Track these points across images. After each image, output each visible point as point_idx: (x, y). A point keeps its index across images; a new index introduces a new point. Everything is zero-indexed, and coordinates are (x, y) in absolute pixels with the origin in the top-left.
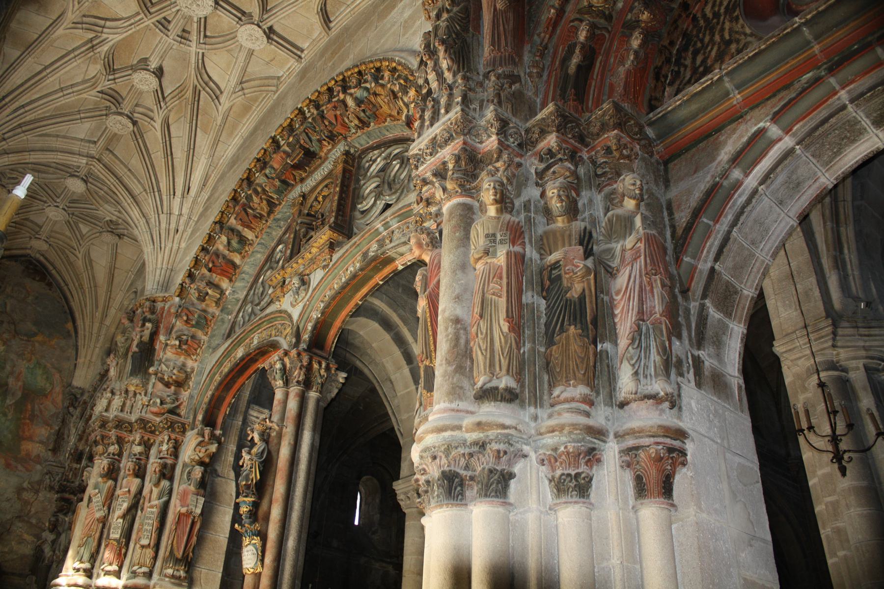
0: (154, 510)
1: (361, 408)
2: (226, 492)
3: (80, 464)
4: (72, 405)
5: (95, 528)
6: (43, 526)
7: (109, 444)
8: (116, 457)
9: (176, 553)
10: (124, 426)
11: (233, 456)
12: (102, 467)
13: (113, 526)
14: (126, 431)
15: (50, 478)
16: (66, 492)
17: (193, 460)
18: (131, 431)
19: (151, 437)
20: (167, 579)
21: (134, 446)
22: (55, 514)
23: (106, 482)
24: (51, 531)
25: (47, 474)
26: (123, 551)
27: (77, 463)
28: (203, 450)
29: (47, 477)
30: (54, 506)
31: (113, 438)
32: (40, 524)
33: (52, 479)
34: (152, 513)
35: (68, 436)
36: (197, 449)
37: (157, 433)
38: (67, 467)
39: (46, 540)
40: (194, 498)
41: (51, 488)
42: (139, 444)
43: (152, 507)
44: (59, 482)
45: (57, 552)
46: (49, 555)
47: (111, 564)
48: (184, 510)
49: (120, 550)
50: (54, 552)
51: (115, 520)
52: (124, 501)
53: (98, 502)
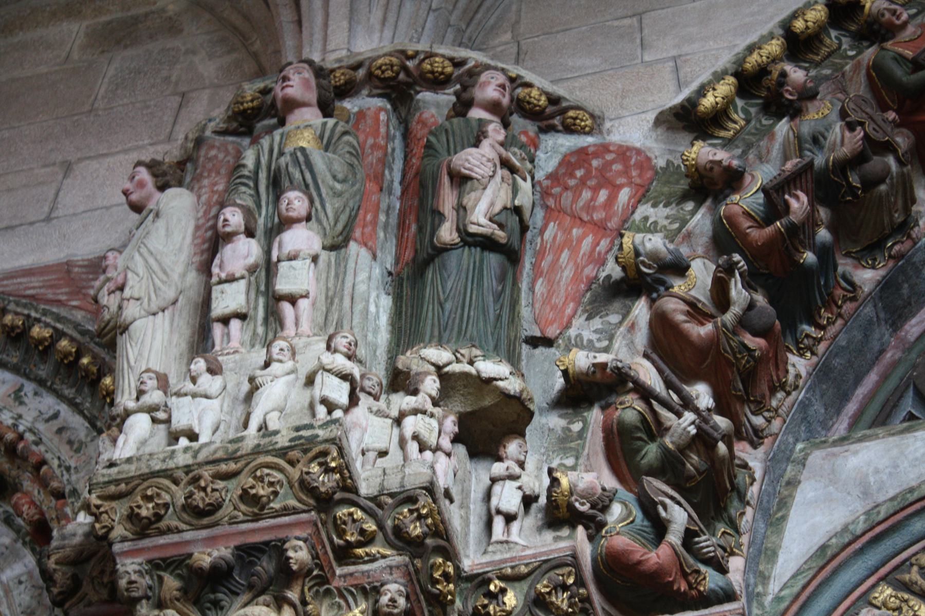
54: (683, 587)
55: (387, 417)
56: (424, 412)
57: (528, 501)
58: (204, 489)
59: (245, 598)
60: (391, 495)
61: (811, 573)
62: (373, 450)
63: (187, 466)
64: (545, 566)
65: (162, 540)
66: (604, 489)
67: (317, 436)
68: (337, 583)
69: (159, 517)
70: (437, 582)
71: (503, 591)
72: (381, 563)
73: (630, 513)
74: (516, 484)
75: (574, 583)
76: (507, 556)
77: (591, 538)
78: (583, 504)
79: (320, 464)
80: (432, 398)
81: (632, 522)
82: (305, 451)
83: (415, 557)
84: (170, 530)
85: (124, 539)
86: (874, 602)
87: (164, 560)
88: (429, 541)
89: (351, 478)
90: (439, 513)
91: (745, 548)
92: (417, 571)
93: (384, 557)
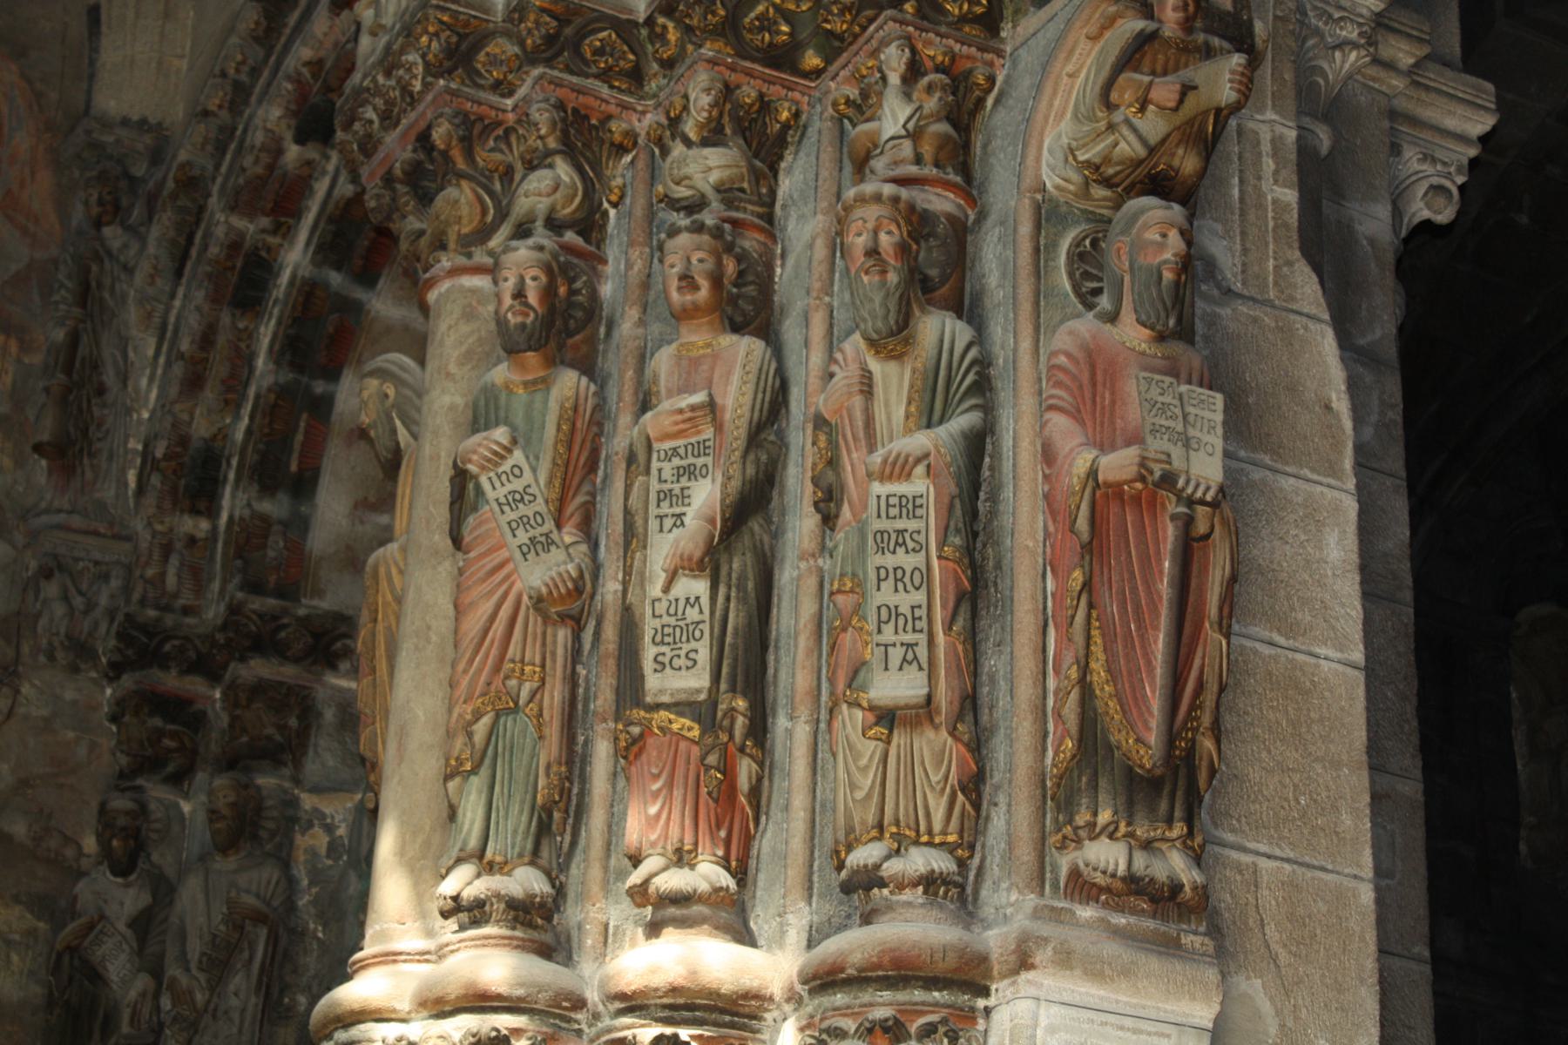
0: (918, 485)
1: (1524, 219)
2: (1293, 389)
3: (212, 513)
4: (112, 211)
5: (533, 653)
6: (70, 852)
7: (508, 174)
8: (570, 237)
9: (1121, 738)
10: (596, 40)
11: (1290, 173)
12: (509, 286)
13: (649, 626)
14: (605, 76)
15: (66, 598)
16: (163, 661)
17: (1096, 172)
18: (636, 76)
19: (775, 91)
20: (1086, 913)
21: (678, 149)
22: (124, 779)
23: (545, 383)
24: (123, 868)
25: (47, 573)
26: (745, 770)
27: (195, 512)
28: (1165, 91)
29: (51, 589)
30: (107, 743)
31: (542, 116)
32: (53, 843)
33: (78, 602)
34: (910, 506)
35: (124, 378)
36: (1125, 94)
37: (812, 60)
38: (145, 537)
39: (102, 917)
40: (1166, 391)
41: (81, 650)
43: (899, 469)
44: (111, 614)
45: (173, 971)
46: (133, 994)
47: (682, 858)
48: (1118, 464)
49: (728, 770)
50: (157, 972)
51: (655, 590)
52: (690, 472)
53: (518, 498)
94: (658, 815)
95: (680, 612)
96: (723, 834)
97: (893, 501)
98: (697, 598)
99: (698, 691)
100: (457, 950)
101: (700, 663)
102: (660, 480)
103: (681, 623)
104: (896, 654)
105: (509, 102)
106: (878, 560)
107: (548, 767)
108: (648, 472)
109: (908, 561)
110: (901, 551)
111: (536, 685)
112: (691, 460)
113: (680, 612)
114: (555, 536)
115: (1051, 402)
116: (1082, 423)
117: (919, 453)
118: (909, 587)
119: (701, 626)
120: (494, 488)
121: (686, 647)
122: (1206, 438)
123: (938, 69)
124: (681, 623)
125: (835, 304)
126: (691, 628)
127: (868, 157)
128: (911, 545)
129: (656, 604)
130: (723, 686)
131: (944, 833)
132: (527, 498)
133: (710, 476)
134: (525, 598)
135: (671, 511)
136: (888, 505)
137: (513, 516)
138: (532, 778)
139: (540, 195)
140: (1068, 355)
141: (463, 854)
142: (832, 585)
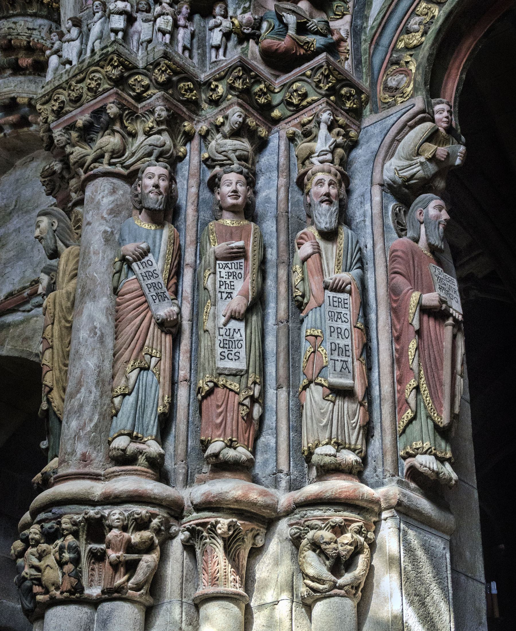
14: (184, 103)
37: (276, 113)
42: (235, 134)
47: (231, 445)
54: (302, 52)
55: (150, 21)
56: (163, 14)
57: (227, 35)
58: (73, 90)
59: (100, 134)
60: (151, 64)
61: (385, 9)
62: (145, 41)
63: (66, 81)
64: (231, 70)
65: (66, 118)
66: (255, 19)
67: (108, 51)
68: (140, 111)
69: (61, 108)
70: (184, 95)
71: (217, 86)
72: (154, 97)
73: (270, 25)
74: (219, 29)
75: (243, 74)
76: (216, 68)
77: (257, 43)
78: (248, 29)
79: (112, 65)
80: (169, 4)
81: (272, 30)
82: (105, 60)
83: (167, 90)
84: (67, 112)
85: (53, 121)
86: (417, 13)
87: (69, 126)
88: (174, 79)
89: (130, 63)
90: (174, 64)
91: (351, 10)
92: (171, 95)
93: (154, 94)
94: (221, 423)
95: (231, 335)
96: (247, 435)
97: (335, 299)
98: (239, 330)
99: (241, 371)
100: (119, 475)
101: (241, 358)
102: (220, 277)
103: (232, 340)
104: (339, 365)
105: (139, 106)
106: (329, 323)
107: (163, 397)
108: (215, 273)
109: (344, 326)
110: (339, 321)
111: (158, 359)
112: (235, 271)
113: (231, 335)
114: (167, 294)
115: (396, 270)
116: (410, 281)
117: (348, 281)
118: (343, 337)
119: (241, 342)
120: (140, 269)
121: (234, 351)
122: (455, 296)
123: (340, 126)
124: (232, 340)
125: (290, 215)
126: (236, 343)
127: (309, 157)
128: (344, 319)
129: (221, 330)
130: (251, 370)
131: (356, 444)
132: (154, 275)
133: (243, 279)
134: (153, 320)
135: (226, 291)
136: (333, 301)
137: (150, 282)
138: (156, 400)
139: (156, 146)
140: (403, 252)
141: (123, 432)
142: (307, 332)
